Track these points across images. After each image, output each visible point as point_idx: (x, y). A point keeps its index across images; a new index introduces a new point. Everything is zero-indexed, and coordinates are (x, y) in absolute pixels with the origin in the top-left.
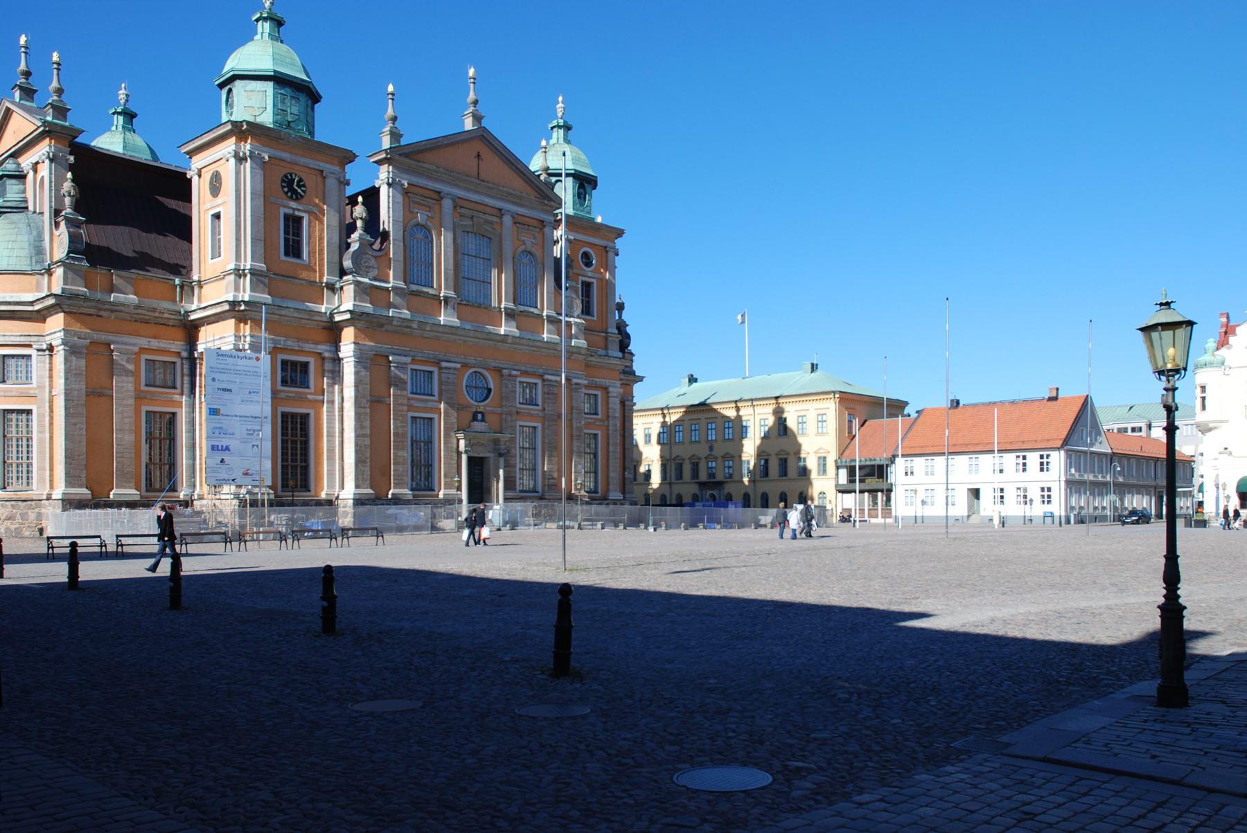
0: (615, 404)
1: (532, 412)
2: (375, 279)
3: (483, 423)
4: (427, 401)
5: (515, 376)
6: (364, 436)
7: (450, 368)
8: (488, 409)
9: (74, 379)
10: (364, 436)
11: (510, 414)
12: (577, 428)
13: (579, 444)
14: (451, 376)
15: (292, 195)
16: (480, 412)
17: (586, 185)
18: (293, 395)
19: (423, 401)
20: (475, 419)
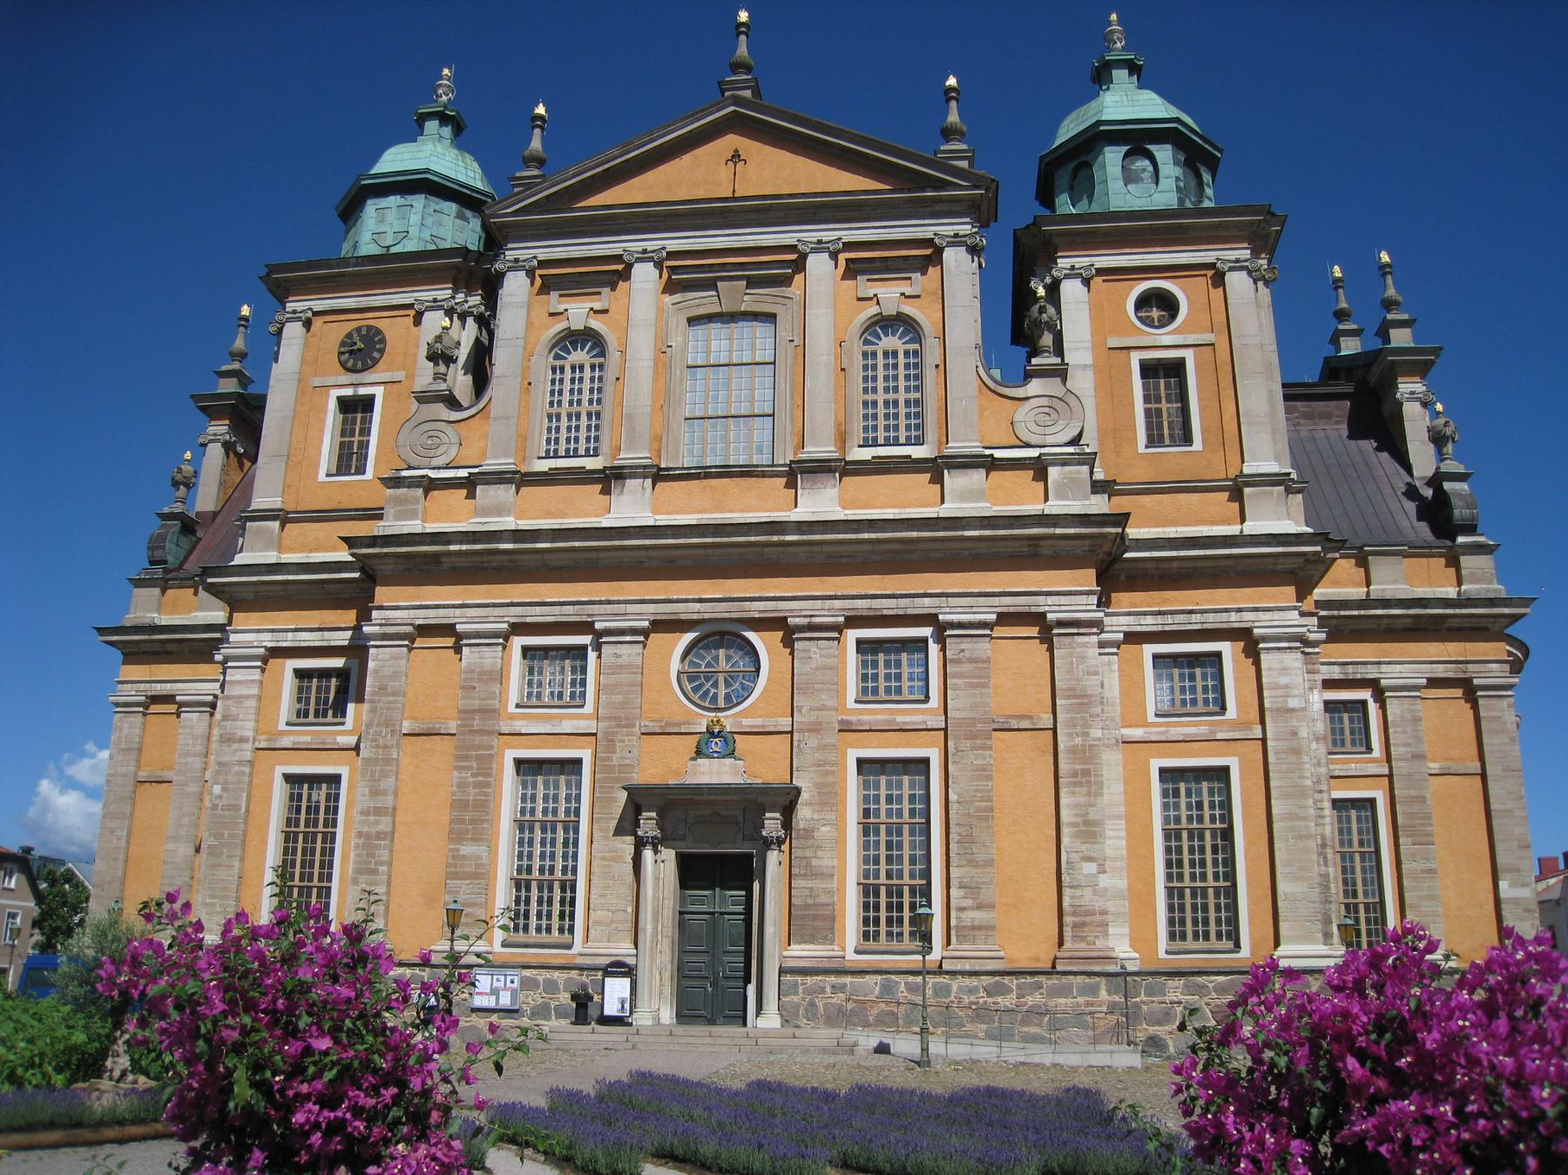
0: (1284, 670)
1: (899, 719)
2: (447, 467)
3: (728, 761)
4: (562, 717)
5: (838, 628)
6: (378, 811)
7: (622, 632)
8: (748, 723)
9: (120, 758)
10: (378, 811)
11: (816, 728)
12: (1072, 751)
13: (1082, 800)
14: (624, 649)
15: (347, 361)
16: (719, 734)
17: (1151, 147)
18: (308, 739)
19: (555, 716)
20: (699, 753)
